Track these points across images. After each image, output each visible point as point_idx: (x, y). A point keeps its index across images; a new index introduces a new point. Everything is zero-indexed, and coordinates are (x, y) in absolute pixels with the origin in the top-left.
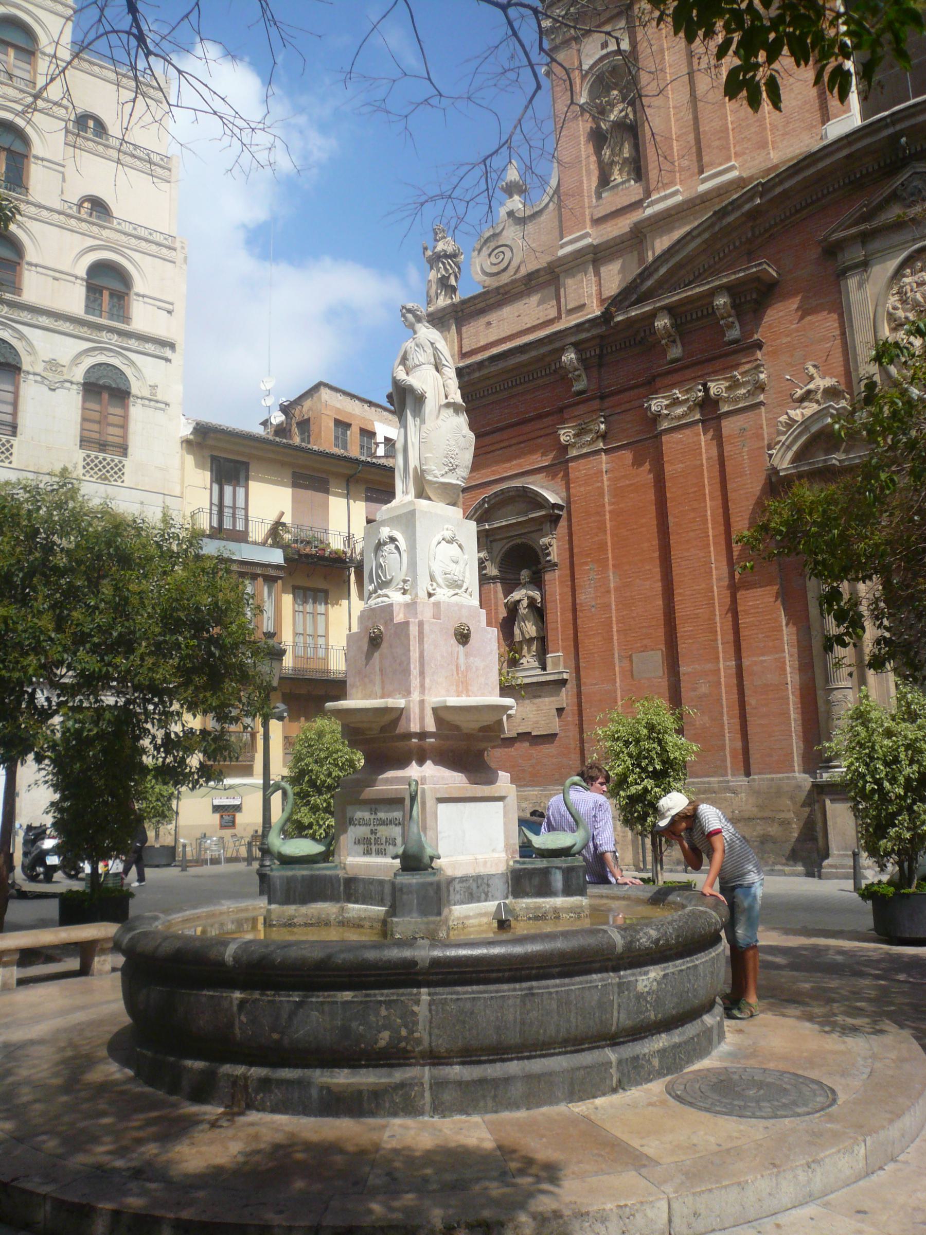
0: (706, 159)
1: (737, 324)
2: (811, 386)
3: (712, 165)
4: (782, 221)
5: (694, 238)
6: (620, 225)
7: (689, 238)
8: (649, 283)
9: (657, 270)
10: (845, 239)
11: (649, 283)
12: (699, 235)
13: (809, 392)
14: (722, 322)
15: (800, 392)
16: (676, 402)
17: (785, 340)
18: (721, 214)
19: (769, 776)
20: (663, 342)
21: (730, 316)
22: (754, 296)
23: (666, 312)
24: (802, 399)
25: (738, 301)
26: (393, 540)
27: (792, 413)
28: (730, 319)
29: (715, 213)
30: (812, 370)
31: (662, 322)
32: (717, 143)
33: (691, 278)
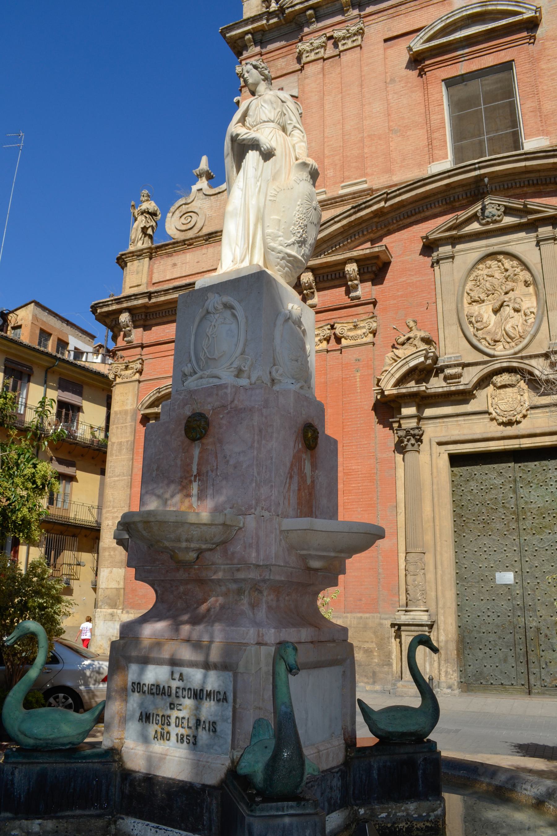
2: (411, 335)
3: (349, 178)
10: (440, 239)
14: (350, 283)
15: (402, 339)
17: (392, 302)
18: (358, 208)
19: (359, 615)
21: (356, 280)
24: (403, 344)
25: (362, 271)
28: (356, 282)
29: (353, 208)
30: (412, 324)
32: (354, 164)
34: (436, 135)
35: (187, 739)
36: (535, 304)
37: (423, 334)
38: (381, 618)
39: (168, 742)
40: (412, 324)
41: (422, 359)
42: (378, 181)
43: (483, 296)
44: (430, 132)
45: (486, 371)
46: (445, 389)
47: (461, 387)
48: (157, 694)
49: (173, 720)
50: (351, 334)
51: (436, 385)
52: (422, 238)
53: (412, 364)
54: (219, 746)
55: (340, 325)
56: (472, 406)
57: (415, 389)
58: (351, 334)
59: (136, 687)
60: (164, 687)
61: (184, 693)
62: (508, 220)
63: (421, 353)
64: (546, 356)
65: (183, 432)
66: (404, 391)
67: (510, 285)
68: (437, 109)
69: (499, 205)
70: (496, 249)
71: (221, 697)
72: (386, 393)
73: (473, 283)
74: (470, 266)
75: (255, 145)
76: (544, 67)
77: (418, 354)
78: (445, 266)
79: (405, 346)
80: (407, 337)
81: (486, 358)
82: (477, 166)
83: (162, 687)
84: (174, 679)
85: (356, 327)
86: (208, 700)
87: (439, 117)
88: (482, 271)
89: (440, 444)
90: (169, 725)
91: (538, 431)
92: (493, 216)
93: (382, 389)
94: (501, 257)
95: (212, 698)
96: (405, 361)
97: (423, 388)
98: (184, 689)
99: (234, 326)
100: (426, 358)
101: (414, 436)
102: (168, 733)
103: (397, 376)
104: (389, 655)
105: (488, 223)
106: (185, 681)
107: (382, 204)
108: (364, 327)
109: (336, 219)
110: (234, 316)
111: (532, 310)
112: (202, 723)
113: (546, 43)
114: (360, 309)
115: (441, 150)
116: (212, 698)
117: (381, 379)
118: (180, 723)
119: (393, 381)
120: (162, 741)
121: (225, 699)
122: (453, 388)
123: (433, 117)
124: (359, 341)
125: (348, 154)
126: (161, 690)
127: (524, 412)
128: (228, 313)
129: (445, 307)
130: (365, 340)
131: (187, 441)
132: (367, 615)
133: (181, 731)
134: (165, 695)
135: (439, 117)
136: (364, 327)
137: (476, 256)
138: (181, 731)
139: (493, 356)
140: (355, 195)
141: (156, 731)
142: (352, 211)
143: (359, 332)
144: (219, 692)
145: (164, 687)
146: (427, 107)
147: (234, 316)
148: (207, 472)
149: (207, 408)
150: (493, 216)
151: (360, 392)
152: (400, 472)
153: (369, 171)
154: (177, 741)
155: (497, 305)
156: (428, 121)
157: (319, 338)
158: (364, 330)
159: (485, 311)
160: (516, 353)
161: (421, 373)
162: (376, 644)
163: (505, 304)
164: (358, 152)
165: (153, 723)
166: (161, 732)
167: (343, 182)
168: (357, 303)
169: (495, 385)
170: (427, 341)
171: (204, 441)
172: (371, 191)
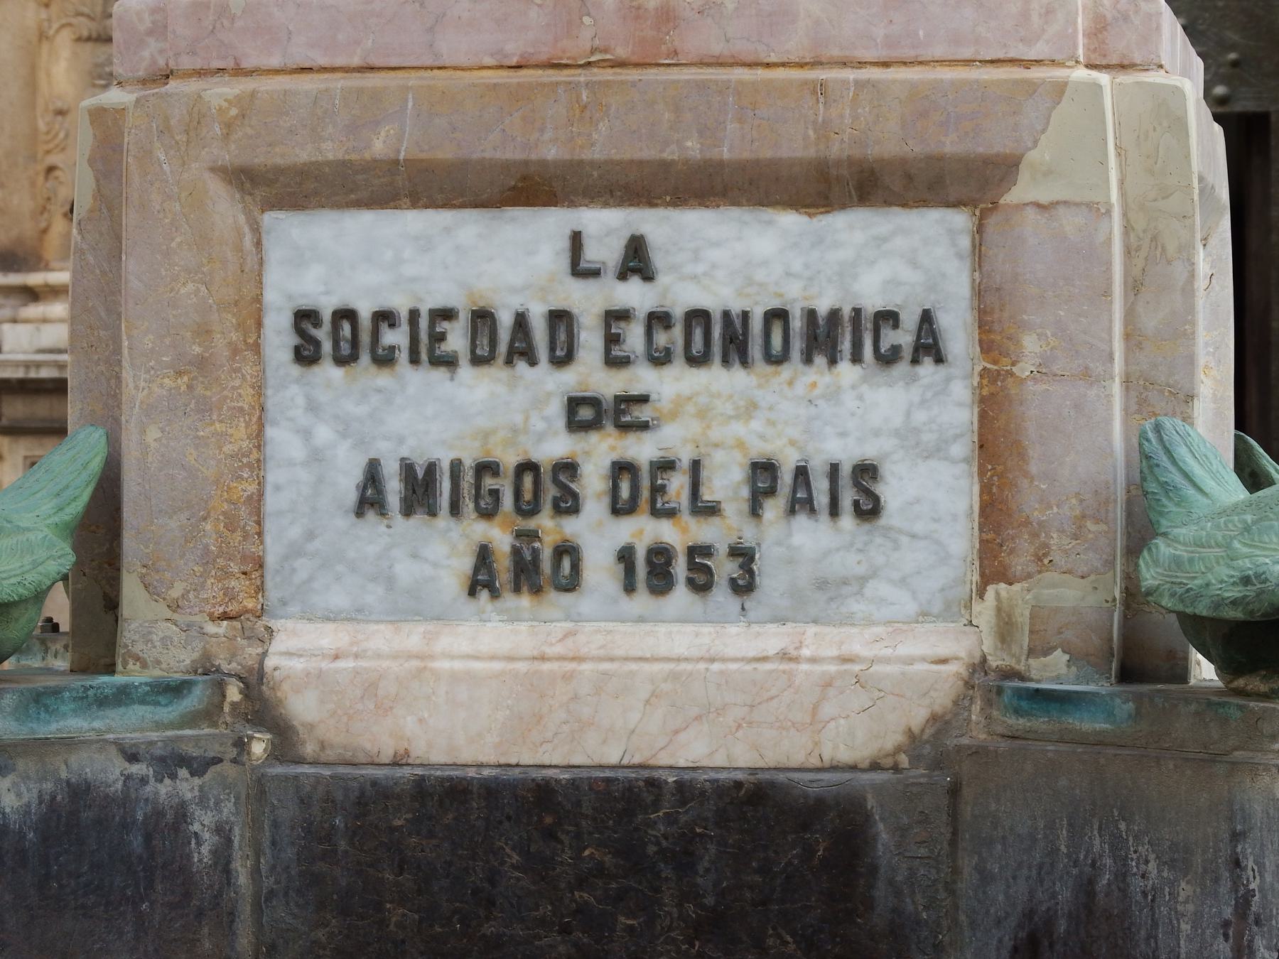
35: (692, 566)
39: (566, 598)
48: (477, 361)
49: (593, 481)
54: (903, 582)
59: (322, 333)
60: (521, 322)
61: (661, 339)
71: (904, 337)
83: (505, 320)
84: (594, 273)
86: (820, 360)
90: (568, 504)
95: (846, 345)
98: (659, 319)
102: (567, 551)
106: (663, 279)
112: (786, 477)
116: (846, 345)
118: (645, 493)
120: (525, 601)
121: (929, 346)
126: (504, 336)
133: (643, 531)
134: (533, 362)
138: (643, 531)
141: (484, 555)
144: (888, 318)
145: (521, 322)
154: (629, 588)
165: (455, 509)
166: (516, 552)
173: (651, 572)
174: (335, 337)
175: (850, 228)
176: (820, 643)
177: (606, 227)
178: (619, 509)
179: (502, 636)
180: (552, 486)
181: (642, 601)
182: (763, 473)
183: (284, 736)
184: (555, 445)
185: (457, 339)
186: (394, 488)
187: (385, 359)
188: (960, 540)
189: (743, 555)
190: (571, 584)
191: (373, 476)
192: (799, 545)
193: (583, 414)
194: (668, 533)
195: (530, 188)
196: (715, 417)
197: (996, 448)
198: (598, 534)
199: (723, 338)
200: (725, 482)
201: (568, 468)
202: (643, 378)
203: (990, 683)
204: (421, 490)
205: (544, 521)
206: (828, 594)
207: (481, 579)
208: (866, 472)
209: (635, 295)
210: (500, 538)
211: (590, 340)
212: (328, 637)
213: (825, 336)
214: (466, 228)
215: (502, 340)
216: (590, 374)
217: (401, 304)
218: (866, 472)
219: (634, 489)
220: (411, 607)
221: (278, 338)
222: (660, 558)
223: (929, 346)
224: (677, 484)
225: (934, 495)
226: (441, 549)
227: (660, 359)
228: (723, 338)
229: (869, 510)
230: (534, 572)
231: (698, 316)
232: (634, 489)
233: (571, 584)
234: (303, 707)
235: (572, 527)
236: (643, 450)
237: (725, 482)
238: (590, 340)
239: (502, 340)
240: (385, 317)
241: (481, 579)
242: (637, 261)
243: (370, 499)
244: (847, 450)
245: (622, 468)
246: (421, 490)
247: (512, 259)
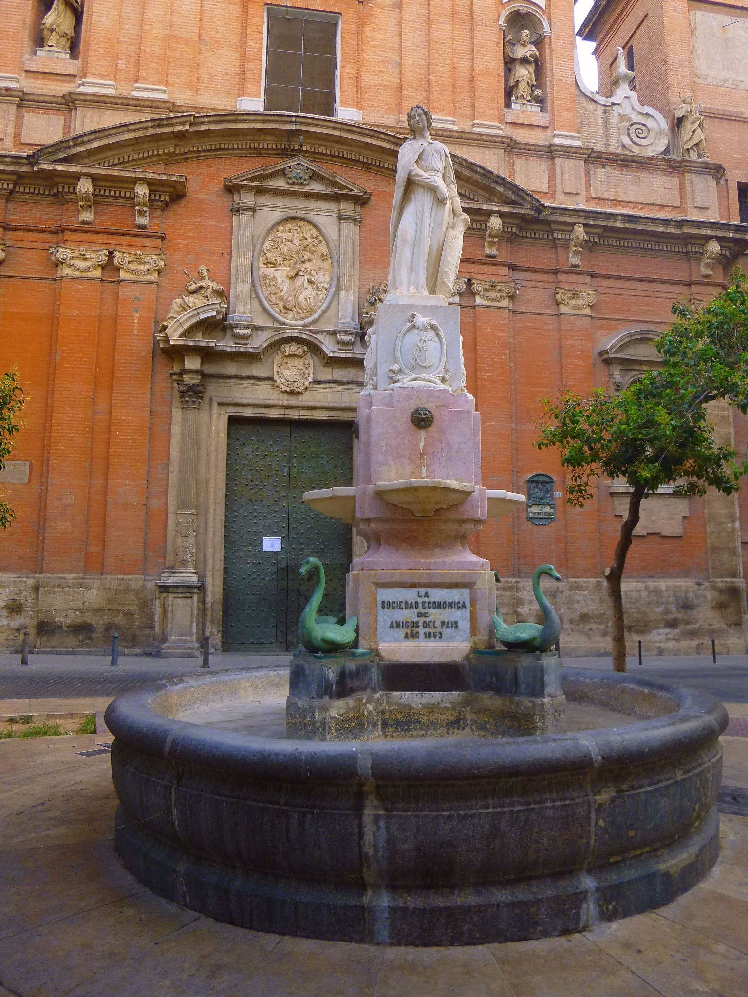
0: (143, 73)
1: (147, 214)
3: (146, 80)
4: (199, 152)
5: (129, 131)
6: (49, 87)
7: (125, 129)
8: (81, 149)
9: (89, 141)
10: (244, 186)
11: (81, 149)
12: (134, 130)
13: (201, 287)
14: (137, 208)
15: (194, 287)
16: (81, 257)
18: (158, 123)
20: (81, 203)
21: (145, 206)
22: (167, 199)
23: (89, 180)
24: (194, 292)
26: (686, 348)
27: (187, 299)
28: (145, 209)
29: (152, 120)
30: (205, 273)
31: (85, 186)
33: (116, 161)
34: (250, 65)
36: (328, 280)
37: (214, 285)
38: (144, 580)
40: (205, 273)
41: (214, 313)
42: (182, 97)
43: (279, 260)
44: (244, 59)
45: (276, 338)
46: (234, 349)
47: (250, 350)
49: (421, 624)
50: (133, 267)
51: (226, 345)
52: (225, 180)
53: (203, 316)
55: (120, 254)
56: (256, 370)
57: (204, 344)
58: (133, 267)
62: (316, 187)
63: (214, 307)
64: (334, 333)
65: (409, 420)
66: (191, 343)
67: (307, 255)
68: (256, 35)
69: (308, 169)
70: (298, 214)
72: (172, 342)
73: (271, 243)
74: (270, 225)
75: (433, 189)
76: (368, 34)
77: (211, 307)
78: (245, 218)
79: (195, 295)
80: (199, 285)
81: (276, 325)
82: (294, 119)
85: (139, 261)
87: (257, 46)
88: (281, 234)
89: (221, 404)
90: (418, 627)
91: (318, 405)
92: (301, 178)
93: (166, 337)
94: (302, 223)
96: (195, 312)
97: (213, 345)
98: (429, 603)
99: (438, 344)
100: (218, 313)
101: (195, 393)
102: (418, 633)
103: (185, 327)
104: (152, 616)
105: (293, 184)
107: (187, 127)
108: (149, 263)
109: (131, 127)
110: (438, 335)
111: (325, 285)
113: (374, 9)
114: (146, 242)
115: (253, 85)
117: (167, 327)
119: (180, 331)
121: (464, 606)
122: (242, 350)
123: (250, 44)
124: (141, 278)
125: (147, 50)
127: (307, 384)
128: (432, 333)
129: (240, 261)
130: (148, 278)
131: (413, 427)
132: (130, 577)
133: (427, 630)
135: (257, 46)
136: (149, 263)
137: (276, 215)
139: (284, 324)
140: (152, 105)
141: (407, 633)
142: (149, 124)
143: (142, 267)
146: (244, 27)
147: (438, 335)
148: (433, 453)
149: (430, 406)
150: (301, 178)
151: (138, 336)
152: (176, 430)
153: (170, 79)
155: (293, 273)
156: (242, 47)
157: (92, 263)
158: (148, 267)
159: (280, 275)
160: (305, 325)
161: (208, 326)
162: (138, 607)
163: (301, 273)
164: (160, 51)
167: (137, 81)
168: (141, 232)
169: (283, 353)
170: (219, 293)
171: (429, 429)
172: (172, 107)
173: (429, 635)
174: (386, 605)
175: (454, 591)
176: (450, 644)
177: (423, 591)
178: (424, 627)
179: (411, 644)
180: (415, 625)
181: (427, 639)
182: (443, 622)
183: (382, 658)
184: (416, 619)
185: (403, 605)
186: (395, 625)
187: (393, 608)
188: (468, 631)
189: (441, 633)
190: (418, 637)
191: (392, 623)
192: (447, 632)
193: (420, 615)
194: (432, 631)
195: (413, 585)
196: (435, 615)
197: (473, 619)
198: (422, 631)
199: (438, 605)
200: (438, 624)
201: (418, 622)
202: (427, 610)
203: (475, 650)
204: (398, 625)
205: (414, 629)
206: (451, 639)
207: (406, 637)
208: (456, 622)
209: (426, 599)
210: (409, 631)
211: (420, 605)
212: (386, 645)
213: (451, 605)
214: (404, 590)
215: (409, 605)
216: (421, 610)
217: (396, 601)
218: (456, 622)
219: (426, 625)
220: (398, 640)
221: (379, 606)
222: (430, 634)
223: (464, 606)
224: (432, 624)
225: (465, 625)
226: (401, 633)
227: (429, 608)
228: (438, 605)
229: (457, 627)
230: (413, 636)
231: (434, 602)
232: (426, 625)
233: (418, 637)
234: (383, 654)
235: (418, 630)
236: (427, 620)
237: (438, 624)
238: (420, 605)
239: (409, 605)
240: (394, 602)
241: (406, 637)
242: (426, 595)
243: (391, 626)
244: (452, 619)
245: (425, 622)
246: (398, 625)
247: (410, 595)
